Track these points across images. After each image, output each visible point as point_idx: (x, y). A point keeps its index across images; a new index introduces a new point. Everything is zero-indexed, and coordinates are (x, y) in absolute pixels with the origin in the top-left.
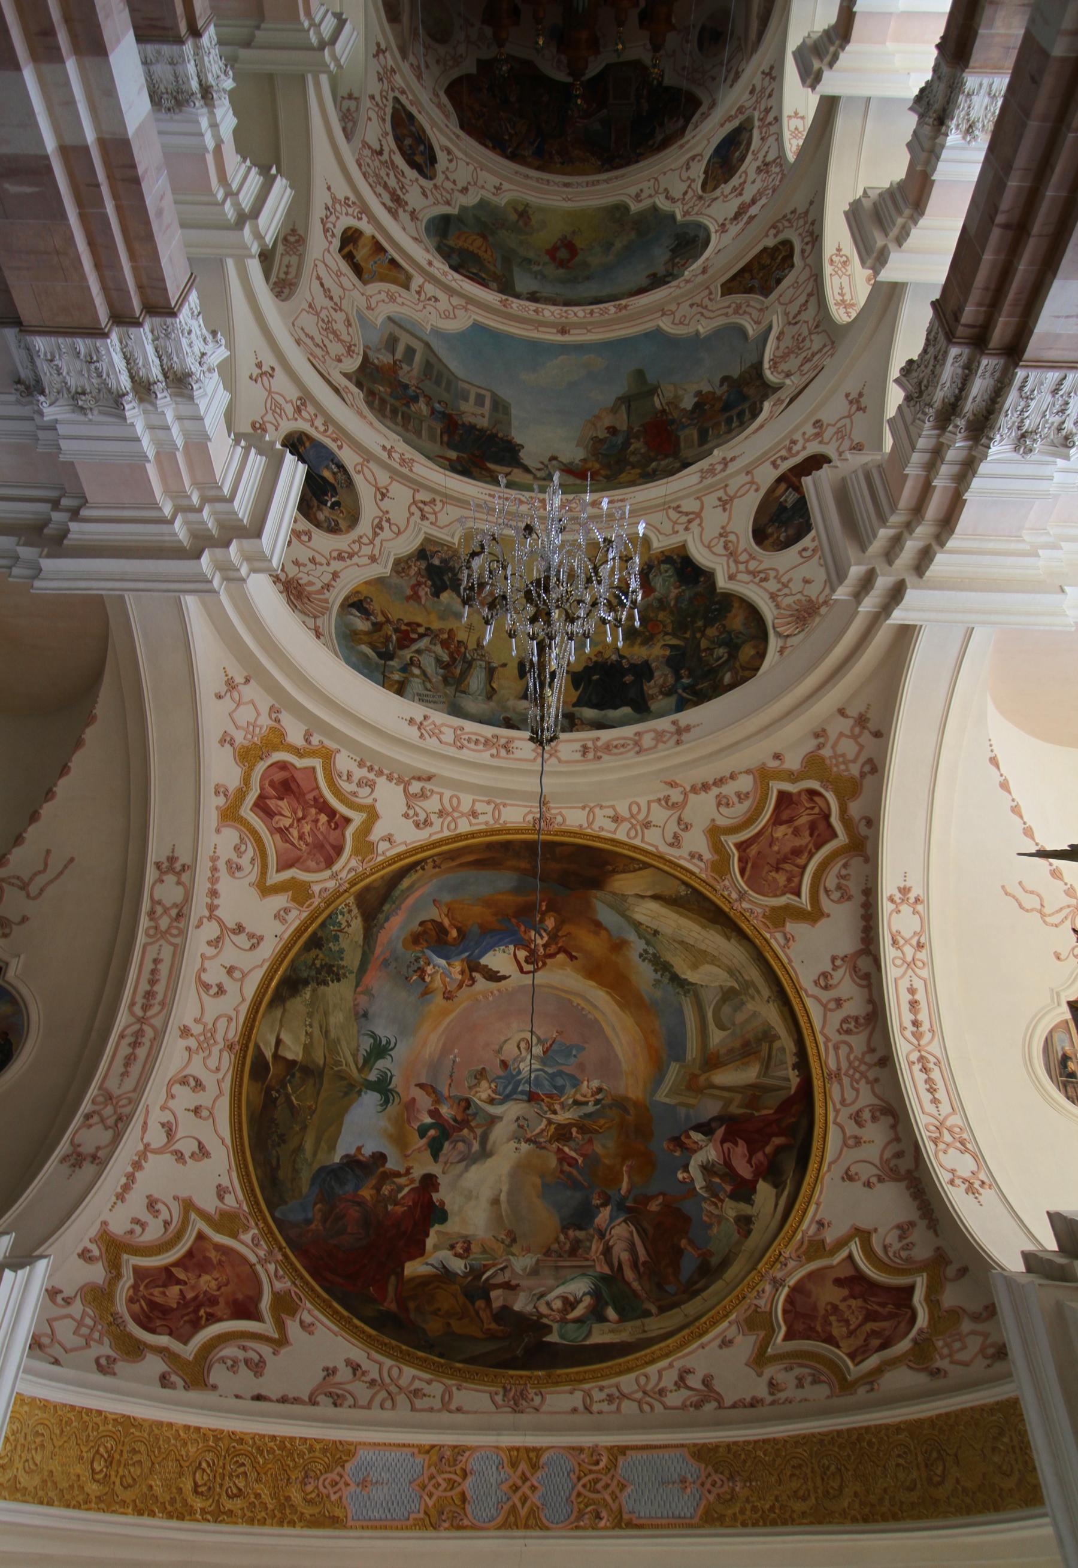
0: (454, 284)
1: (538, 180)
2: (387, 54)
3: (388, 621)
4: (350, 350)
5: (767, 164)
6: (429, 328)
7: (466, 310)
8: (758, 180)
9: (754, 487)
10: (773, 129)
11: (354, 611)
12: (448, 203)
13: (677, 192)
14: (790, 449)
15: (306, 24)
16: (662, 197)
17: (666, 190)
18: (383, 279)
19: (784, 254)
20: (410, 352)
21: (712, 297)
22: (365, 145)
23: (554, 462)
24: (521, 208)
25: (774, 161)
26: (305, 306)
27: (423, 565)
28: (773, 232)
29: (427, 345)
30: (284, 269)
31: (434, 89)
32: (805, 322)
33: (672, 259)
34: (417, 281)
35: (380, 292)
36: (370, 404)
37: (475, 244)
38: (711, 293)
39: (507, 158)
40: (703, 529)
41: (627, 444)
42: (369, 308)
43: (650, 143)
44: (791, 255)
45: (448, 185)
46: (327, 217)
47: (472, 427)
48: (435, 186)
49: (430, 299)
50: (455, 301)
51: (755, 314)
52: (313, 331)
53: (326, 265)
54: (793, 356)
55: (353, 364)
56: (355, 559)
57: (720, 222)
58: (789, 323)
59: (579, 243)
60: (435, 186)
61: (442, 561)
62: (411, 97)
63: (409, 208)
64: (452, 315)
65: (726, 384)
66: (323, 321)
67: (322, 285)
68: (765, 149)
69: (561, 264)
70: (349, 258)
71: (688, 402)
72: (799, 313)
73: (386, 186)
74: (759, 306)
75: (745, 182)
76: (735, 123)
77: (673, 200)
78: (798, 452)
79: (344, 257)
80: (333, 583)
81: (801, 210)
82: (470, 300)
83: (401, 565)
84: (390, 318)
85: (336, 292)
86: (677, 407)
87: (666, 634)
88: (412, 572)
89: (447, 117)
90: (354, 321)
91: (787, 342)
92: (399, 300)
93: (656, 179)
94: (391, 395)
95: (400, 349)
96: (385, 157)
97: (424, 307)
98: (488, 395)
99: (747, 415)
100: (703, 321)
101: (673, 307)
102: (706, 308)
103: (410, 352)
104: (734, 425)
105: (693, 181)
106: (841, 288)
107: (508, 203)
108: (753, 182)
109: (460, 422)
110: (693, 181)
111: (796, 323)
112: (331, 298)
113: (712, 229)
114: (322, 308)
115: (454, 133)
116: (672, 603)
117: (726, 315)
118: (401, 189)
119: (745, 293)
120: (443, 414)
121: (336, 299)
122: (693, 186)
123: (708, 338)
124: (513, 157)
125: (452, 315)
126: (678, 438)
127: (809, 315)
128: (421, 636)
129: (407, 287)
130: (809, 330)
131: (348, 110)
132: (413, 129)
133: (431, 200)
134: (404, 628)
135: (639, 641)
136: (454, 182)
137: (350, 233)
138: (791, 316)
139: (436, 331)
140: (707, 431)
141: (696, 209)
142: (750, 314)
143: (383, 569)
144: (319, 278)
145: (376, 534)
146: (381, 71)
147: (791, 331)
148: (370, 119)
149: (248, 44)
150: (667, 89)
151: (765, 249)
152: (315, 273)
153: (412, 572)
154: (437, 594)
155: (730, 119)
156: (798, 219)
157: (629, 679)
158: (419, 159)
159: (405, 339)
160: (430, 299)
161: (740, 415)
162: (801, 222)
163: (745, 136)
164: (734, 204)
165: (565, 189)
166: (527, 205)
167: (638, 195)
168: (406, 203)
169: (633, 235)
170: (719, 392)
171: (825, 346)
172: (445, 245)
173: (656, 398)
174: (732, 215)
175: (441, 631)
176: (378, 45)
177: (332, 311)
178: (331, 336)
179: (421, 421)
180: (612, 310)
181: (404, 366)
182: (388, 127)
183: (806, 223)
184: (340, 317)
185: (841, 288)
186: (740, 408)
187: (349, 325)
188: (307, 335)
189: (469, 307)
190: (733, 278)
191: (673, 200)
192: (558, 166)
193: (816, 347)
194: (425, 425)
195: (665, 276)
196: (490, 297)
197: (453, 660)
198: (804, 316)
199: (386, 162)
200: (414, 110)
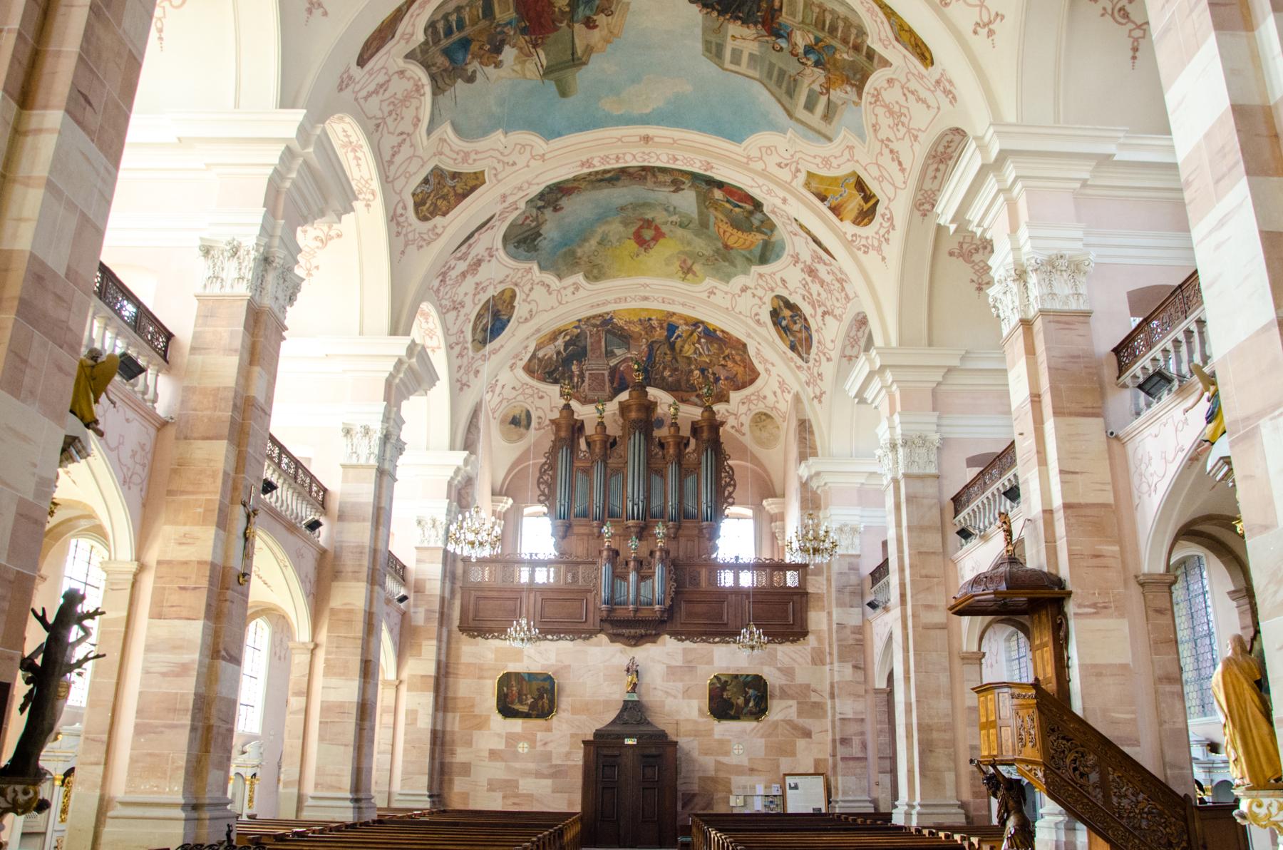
0: (761, 181)
1: (673, 302)
2: (812, 395)
4: (877, 96)
5: (455, 308)
6: (789, 134)
7: (749, 158)
8: (461, 295)
10: (453, 339)
12: (761, 276)
13: (539, 293)
15: (894, 387)
16: (553, 287)
17: (550, 294)
18: (834, 180)
19: (425, 208)
20: (810, 107)
21: (494, 172)
22: (839, 318)
24: (690, 276)
25: (448, 311)
26: (922, 137)
28: (439, 231)
29: (790, 115)
30: (939, 175)
31: (770, 375)
32: (393, 134)
33: (539, 226)
35: (839, 166)
36: (862, 32)
37: (736, 238)
38: (495, 175)
39: (702, 322)
42: (851, 148)
43: (568, 338)
44: (418, 205)
45: (760, 292)
46: (888, 232)
47: (745, 22)
48: (772, 290)
49: (786, 165)
50: (759, 166)
51: (446, 150)
52: (917, 110)
53: (893, 185)
54: (399, 96)
55: (877, 79)
57: (494, 259)
58: (408, 134)
59: (632, 245)
62: (792, 364)
63: (800, 265)
64: (764, 150)
65: (469, 74)
66: (903, 124)
67: (900, 164)
68: (459, 322)
69: (648, 223)
70: (867, 196)
71: (509, 54)
72: (400, 145)
73: (822, 283)
74: (443, 157)
75: (475, 295)
76: (489, 347)
77: (543, 284)
79: (874, 196)
81: (412, 249)
82: (745, 166)
84: (830, 140)
85: (886, 160)
86: (521, 49)
89: (758, 352)
90: (869, 132)
91: (409, 114)
92: (818, 161)
93: (560, 303)
94: (835, 49)
96: (820, 311)
97: (792, 156)
99: (441, 26)
100: (501, 148)
101: (533, 163)
103: (810, 107)
104: (453, 18)
105: (524, 301)
106: (358, 165)
108: (466, 294)
109: (759, 26)
110: (524, 301)
111: (402, 134)
112: (891, 151)
114: (903, 139)
115: (753, 338)
117: (477, 153)
118: (807, 283)
119: (460, 173)
120: (779, 36)
121: (886, 151)
123: (493, 128)
124: (697, 323)
125: (764, 150)
126: (517, 10)
127: (389, 141)
129: (810, 174)
130: (385, 123)
131: (853, 347)
132: (792, 338)
133: (777, 278)
136: (754, 296)
137: (866, 220)
138: (408, 143)
139: (783, 131)
140: (485, 16)
141: (519, 275)
142: (451, 150)
144: (903, 170)
146: (819, 381)
147: (406, 126)
148: (832, 341)
149: (950, 370)
150: (556, 382)
151: (444, 214)
152: (906, 174)
155: (495, 352)
156: (415, 240)
158: (787, 313)
159: (815, 119)
160: (786, 165)
161: (449, 32)
162: (411, 236)
163: (479, 336)
164: (485, 272)
165: (647, 294)
167: (577, 289)
168: (802, 270)
169: (579, 252)
170: (474, 65)
171: (366, 98)
172: (765, 234)
173: (545, 63)
174: (484, 265)
176: (820, 402)
177: (892, 138)
178: (896, 108)
179: (803, 22)
180: (596, 162)
181: (818, 89)
182: (815, 337)
183: (406, 235)
184: (883, 134)
185: (358, 165)
186: (450, 41)
187: (874, 126)
188: (924, 101)
189: (745, 160)
190: (473, 189)
191: (543, 284)
192: (653, 317)
193: (375, 100)
194: (799, 18)
195: (544, 207)
196: (722, 173)
198: (395, 140)
199: (819, 306)
200: (790, 354)
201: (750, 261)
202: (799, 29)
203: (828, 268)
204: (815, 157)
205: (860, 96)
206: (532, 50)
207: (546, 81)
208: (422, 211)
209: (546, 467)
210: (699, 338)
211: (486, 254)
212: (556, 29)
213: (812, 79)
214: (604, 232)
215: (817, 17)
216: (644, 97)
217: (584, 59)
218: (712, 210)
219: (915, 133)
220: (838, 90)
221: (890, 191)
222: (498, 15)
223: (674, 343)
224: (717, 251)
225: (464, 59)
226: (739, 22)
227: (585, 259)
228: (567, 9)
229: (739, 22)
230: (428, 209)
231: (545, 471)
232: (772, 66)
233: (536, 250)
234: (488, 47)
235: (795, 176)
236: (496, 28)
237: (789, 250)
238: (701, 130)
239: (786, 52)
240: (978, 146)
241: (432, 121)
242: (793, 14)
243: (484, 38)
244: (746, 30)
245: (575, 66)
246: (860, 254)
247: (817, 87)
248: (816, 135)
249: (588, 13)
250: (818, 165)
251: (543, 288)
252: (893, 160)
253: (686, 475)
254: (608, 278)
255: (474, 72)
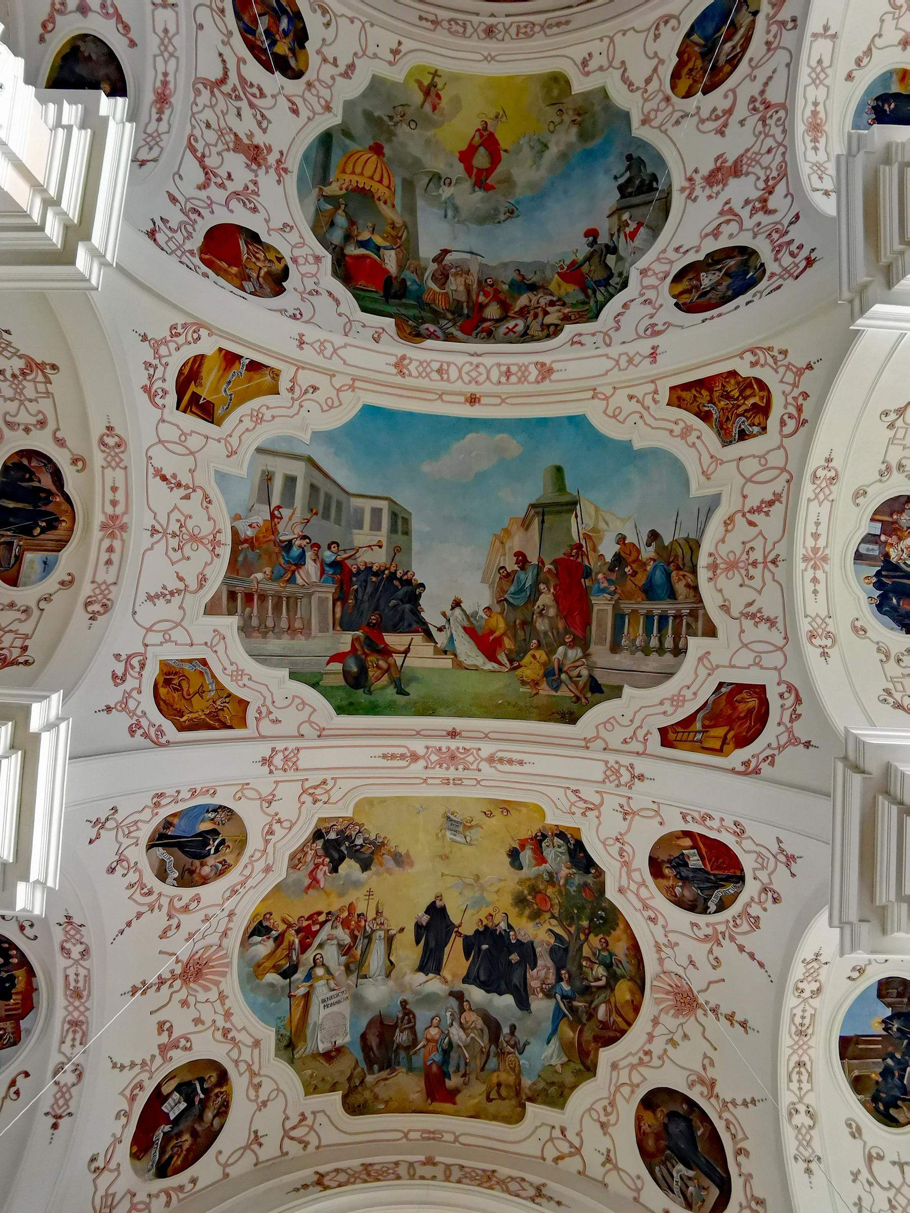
3: (290, 926)
9: (659, 819)
10: (788, 38)
11: (256, 939)
13: (639, 71)
14: (704, 819)
16: (617, 74)
17: (623, 63)
18: (244, 398)
20: (291, 481)
23: (457, 611)
27: (320, 843)
28: (749, 357)
29: (311, 461)
34: (287, 373)
40: (600, 823)
41: (536, 593)
44: (764, 410)
45: (328, 71)
47: (369, 569)
56: (250, 883)
60: (309, 85)
61: (340, 833)
64: (336, 403)
65: (654, 544)
67: (164, 478)
71: (608, 549)
78: (711, 828)
79: (185, 411)
80: (231, 925)
83: (296, 860)
86: (595, 549)
87: (553, 917)
88: (309, 857)
93: (612, 40)
95: (278, 485)
98: (384, 505)
100: (640, 422)
101: (608, 391)
102: (647, 409)
103: (291, 481)
107: (410, 74)
110: (661, 62)
113: (676, 187)
116: (562, 882)
119: (698, 415)
122: (661, 69)
127: (770, 524)
128: (322, 924)
134: (305, 923)
135: (527, 912)
136: (335, 63)
137: (186, 371)
139: (315, 434)
141: (661, 116)
143: (281, 873)
145: (267, 842)
152: (151, 470)
153: (309, 857)
154: (335, 870)
157: (514, 958)
166: (435, 74)
167: (585, 63)
174: (705, 170)
175: (341, 910)
179: (310, 595)
183: (795, 385)
189: (357, 384)
197: (354, 938)
199: (234, 89)
201: (345, 131)
202: (314, 584)
203: (231, 187)
204: (273, 417)
205: (235, 532)
206: (583, 543)
207: (576, 494)
208: (762, 398)
211: (698, 191)
212: (555, 562)
213: (293, 521)
214: (538, 168)
215: (296, 614)
216: (473, 454)
217: (533, 512)
218: (399, 222)
219: (157, 537)
220: (261, 523)
221: (169, 433)
222: (610, 608)
224: (391, 135)
225: (655, 568)
226: (375, 568)
227: (567, 119)
228: (542, 586)
229: (375, 568)
230: (753, 395)
232: (338, 522)
233: (629, 158)
234: (626, 570)
235: (293, 380)
236: (615, 592)
237: (291, 181)
238: (411, 414)
239: (324, 546)
240: (104, 256)
241: (710, 512)
242: (322, 601)
243: (629, 585)
244: (368, 560)
245: (544, 506)
246: (180, 320)
247: (286, 512)
248: (276, 448)
249: (522, 576)
250: (268, 408)
251: (632, 78)
252: (174, 476)
254: (539, 76)
255: (649, 545)
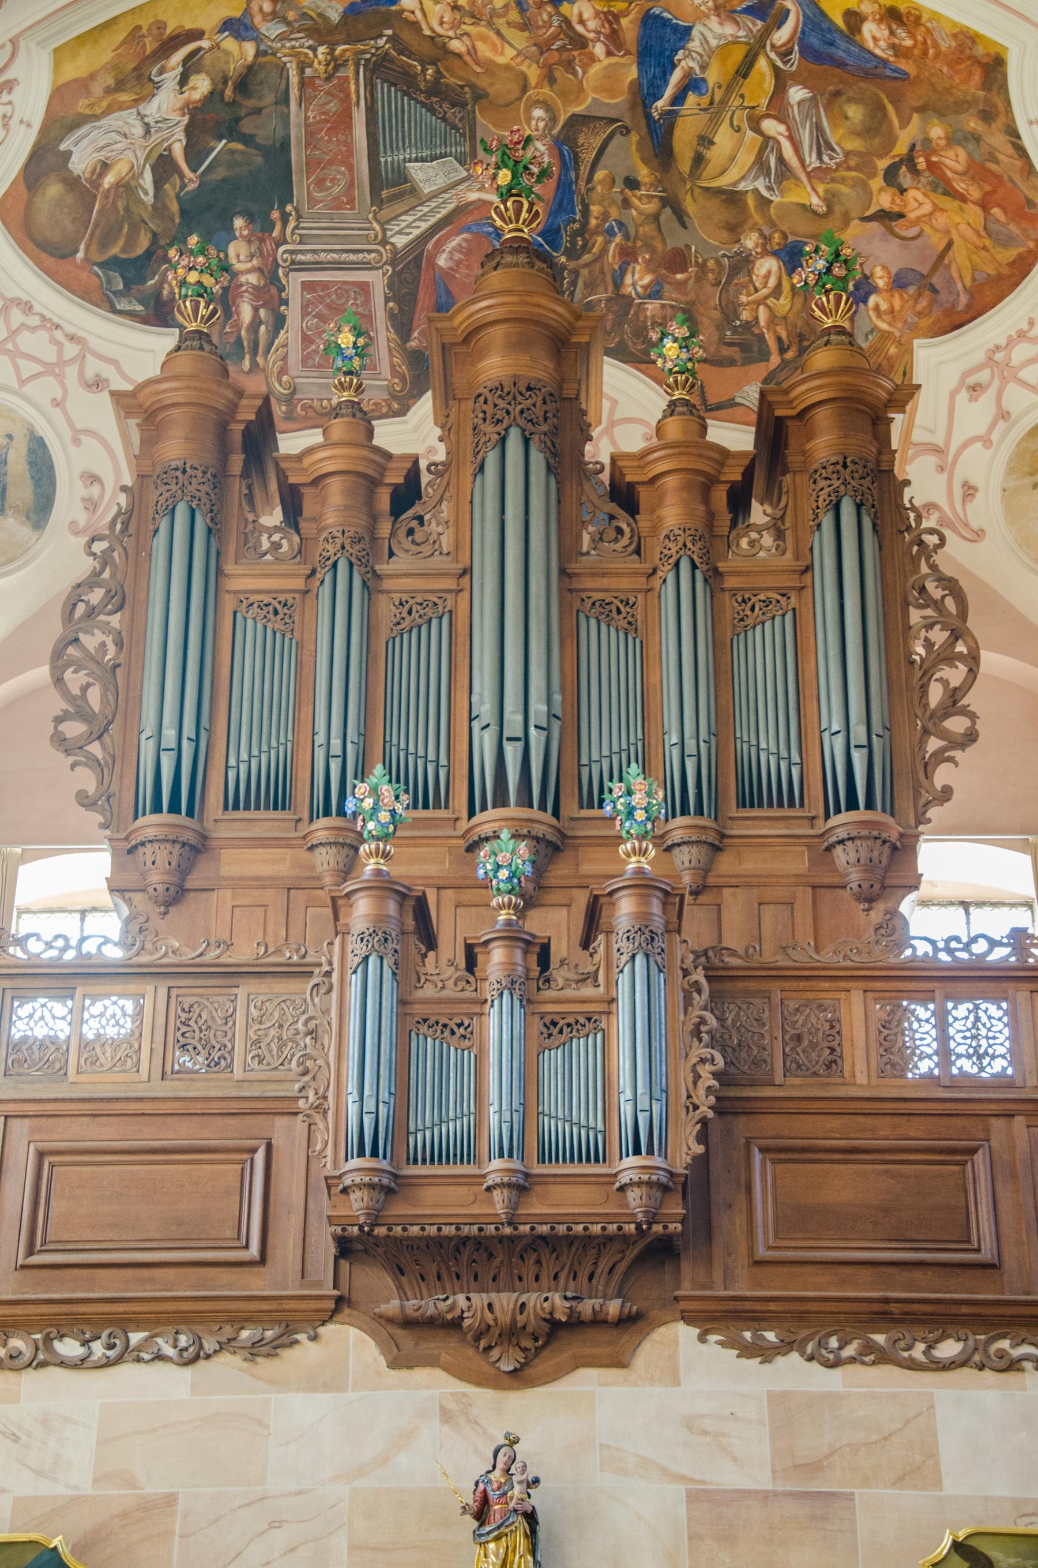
209: (96, 596)
210: (781, 81)
223: (672, 117)
231: (92, 612)
253: (743, 625)
